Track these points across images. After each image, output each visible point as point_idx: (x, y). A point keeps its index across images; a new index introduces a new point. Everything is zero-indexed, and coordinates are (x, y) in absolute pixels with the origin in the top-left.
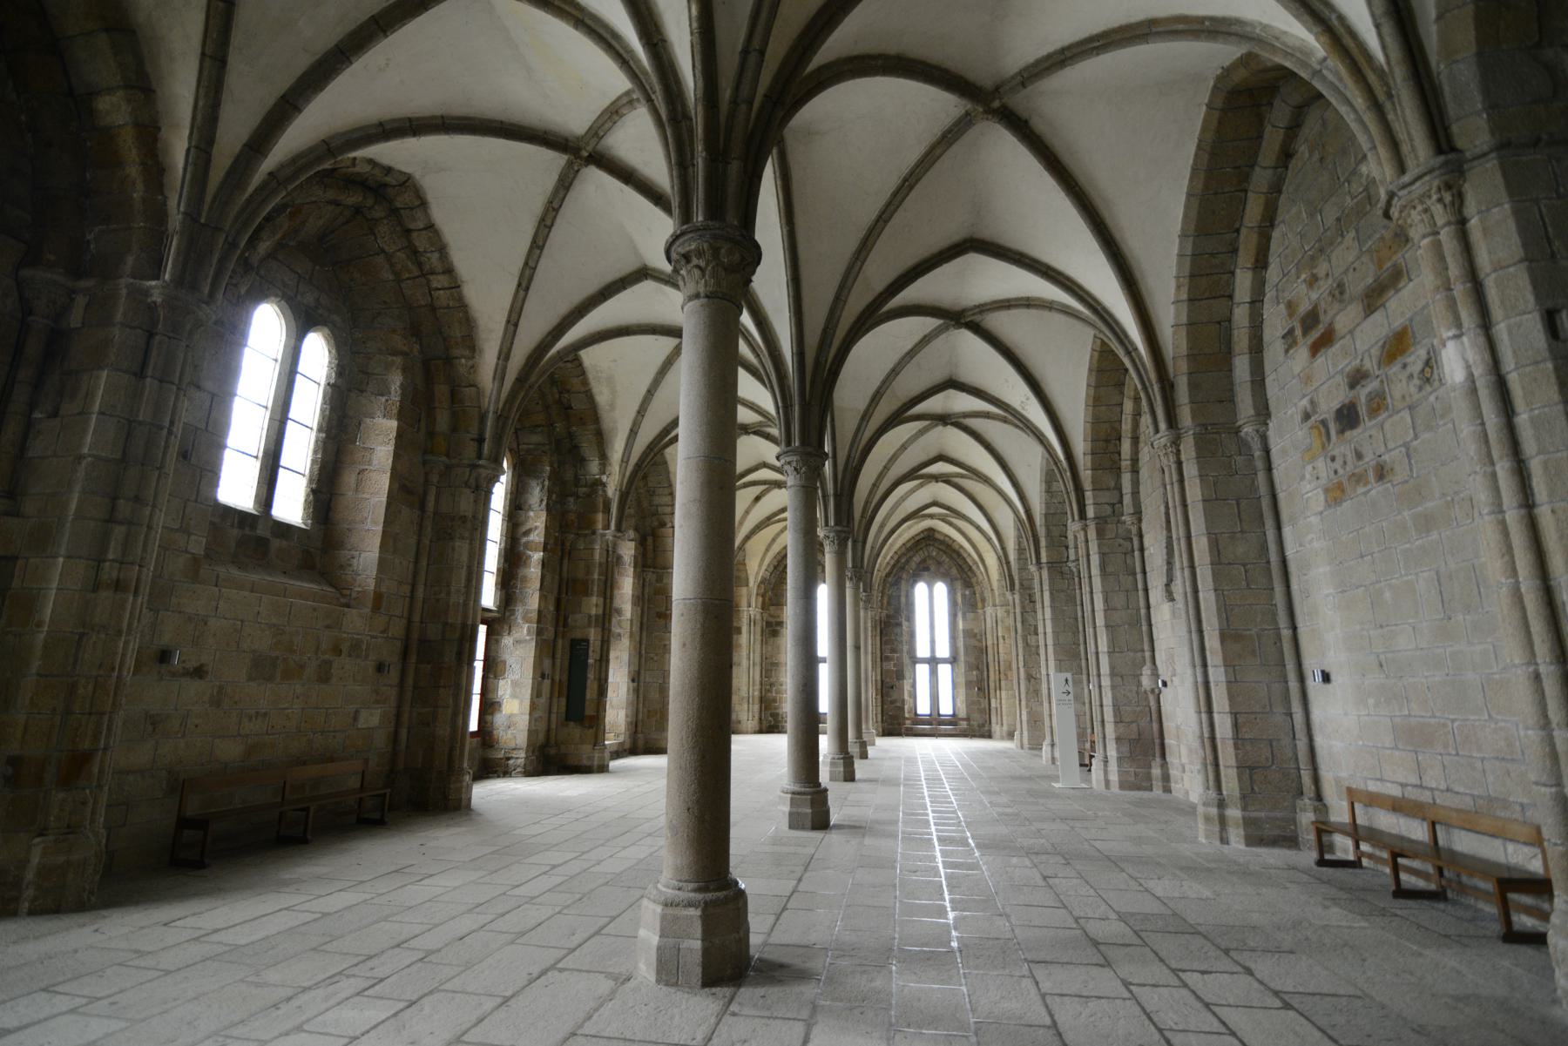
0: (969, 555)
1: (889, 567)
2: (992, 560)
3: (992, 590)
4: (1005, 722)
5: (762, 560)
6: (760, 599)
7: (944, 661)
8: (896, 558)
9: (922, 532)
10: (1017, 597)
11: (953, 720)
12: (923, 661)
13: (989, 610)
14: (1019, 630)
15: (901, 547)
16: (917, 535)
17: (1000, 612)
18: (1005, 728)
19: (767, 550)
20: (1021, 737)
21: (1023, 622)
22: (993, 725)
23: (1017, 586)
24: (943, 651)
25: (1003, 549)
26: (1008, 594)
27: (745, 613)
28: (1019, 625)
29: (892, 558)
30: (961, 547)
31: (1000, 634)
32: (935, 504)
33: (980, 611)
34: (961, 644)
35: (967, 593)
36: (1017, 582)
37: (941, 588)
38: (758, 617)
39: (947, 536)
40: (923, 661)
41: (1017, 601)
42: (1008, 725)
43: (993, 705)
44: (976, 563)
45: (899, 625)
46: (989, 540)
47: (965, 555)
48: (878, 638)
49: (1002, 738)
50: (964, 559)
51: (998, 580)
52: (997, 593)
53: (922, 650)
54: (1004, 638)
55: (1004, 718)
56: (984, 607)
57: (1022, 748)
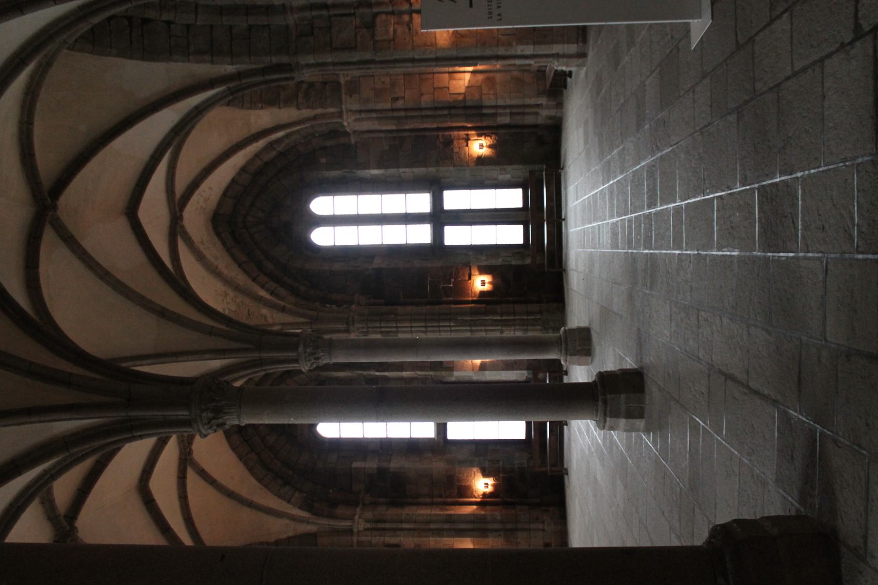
0: (257, 156)
1: (282, 291)
2: (263, 118)
3: (315, 118)
4: (532, 101)
5: (269, 511)
6: (340, 510)
7: (437, 201)
8: (263, 278)
9: (218, 234)
10: (303, 60)
11: (532, 187)
12: (438, 235)
13: (349, 123)
14: (368, 56)
15: (245, 271)
16: (224, 244)
17: (351, 104)
18: (543, 101)
19: (250, 504)
20: (564, 56)
21: (350, 47)
22: (540, 121)
23: (285, 59)
24: (421, 202)
25: (211, 83)
26: (298, 76)
27: (363, 538)
28: (357, 56)
29: (263, 287)
30: (243, 169)
31: (388, 106)
32: (131, 211)
33: (353, 140)
34: (407, 172)
35: (323, 160)
36: (275, 60)
37: (321, 205)
38: (369, 515)
39: (225, 194)
40: (438, 235)
41: (311, 60)
42: (540, 94)
43: (506, 120)
44: (271, 146)
45: (379, 271)
46: (198, 112)
47: (259, 163)
48: (400, 309)
49: (560, 105)
50: (267, 164)
51: (298, 109)
52: (319, 111)
53: (421, 235)
54: (396, 99)
55: (529, 101)
56: (347, 134)
57: (583, 55)
